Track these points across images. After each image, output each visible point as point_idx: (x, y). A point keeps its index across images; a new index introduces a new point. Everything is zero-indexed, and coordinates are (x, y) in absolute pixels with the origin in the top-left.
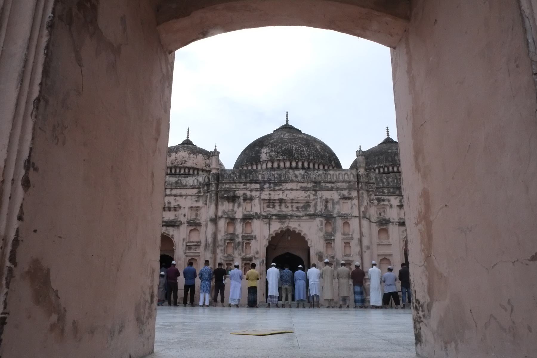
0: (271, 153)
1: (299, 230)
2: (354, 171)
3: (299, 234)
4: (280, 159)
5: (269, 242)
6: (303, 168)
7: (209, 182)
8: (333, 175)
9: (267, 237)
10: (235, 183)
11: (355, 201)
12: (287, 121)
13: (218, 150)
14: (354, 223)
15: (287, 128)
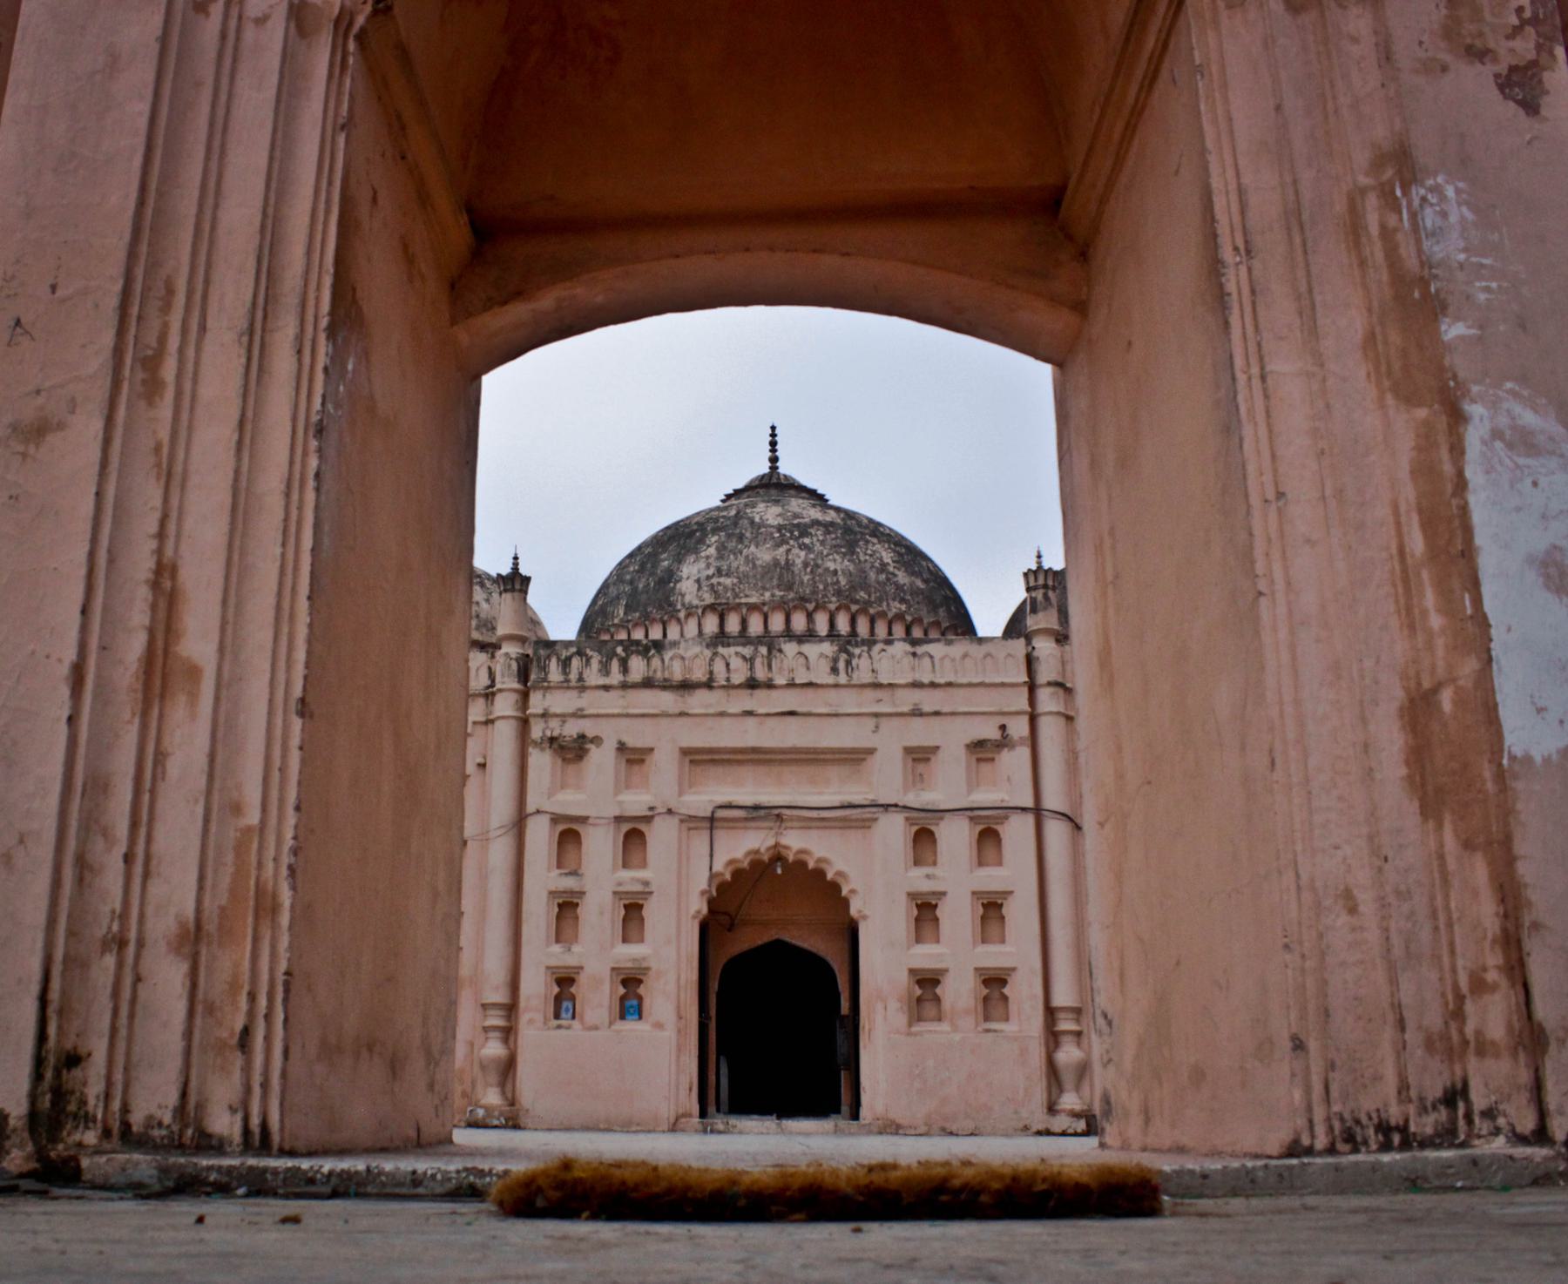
0: (714, 581)
1: (820, 860)
2: (1019, 646)
3: (819, 873)
4: (753, 600)
5: (711, 902)
6: (832, 634)
7: (492, 685)
8: (942, 659)
9: (704, 885)
10: (582, 687)
11: (1024, 753)
12: (774, 460)
13: (523, 571)
14: (1017, 832)
15: (773, 485)
